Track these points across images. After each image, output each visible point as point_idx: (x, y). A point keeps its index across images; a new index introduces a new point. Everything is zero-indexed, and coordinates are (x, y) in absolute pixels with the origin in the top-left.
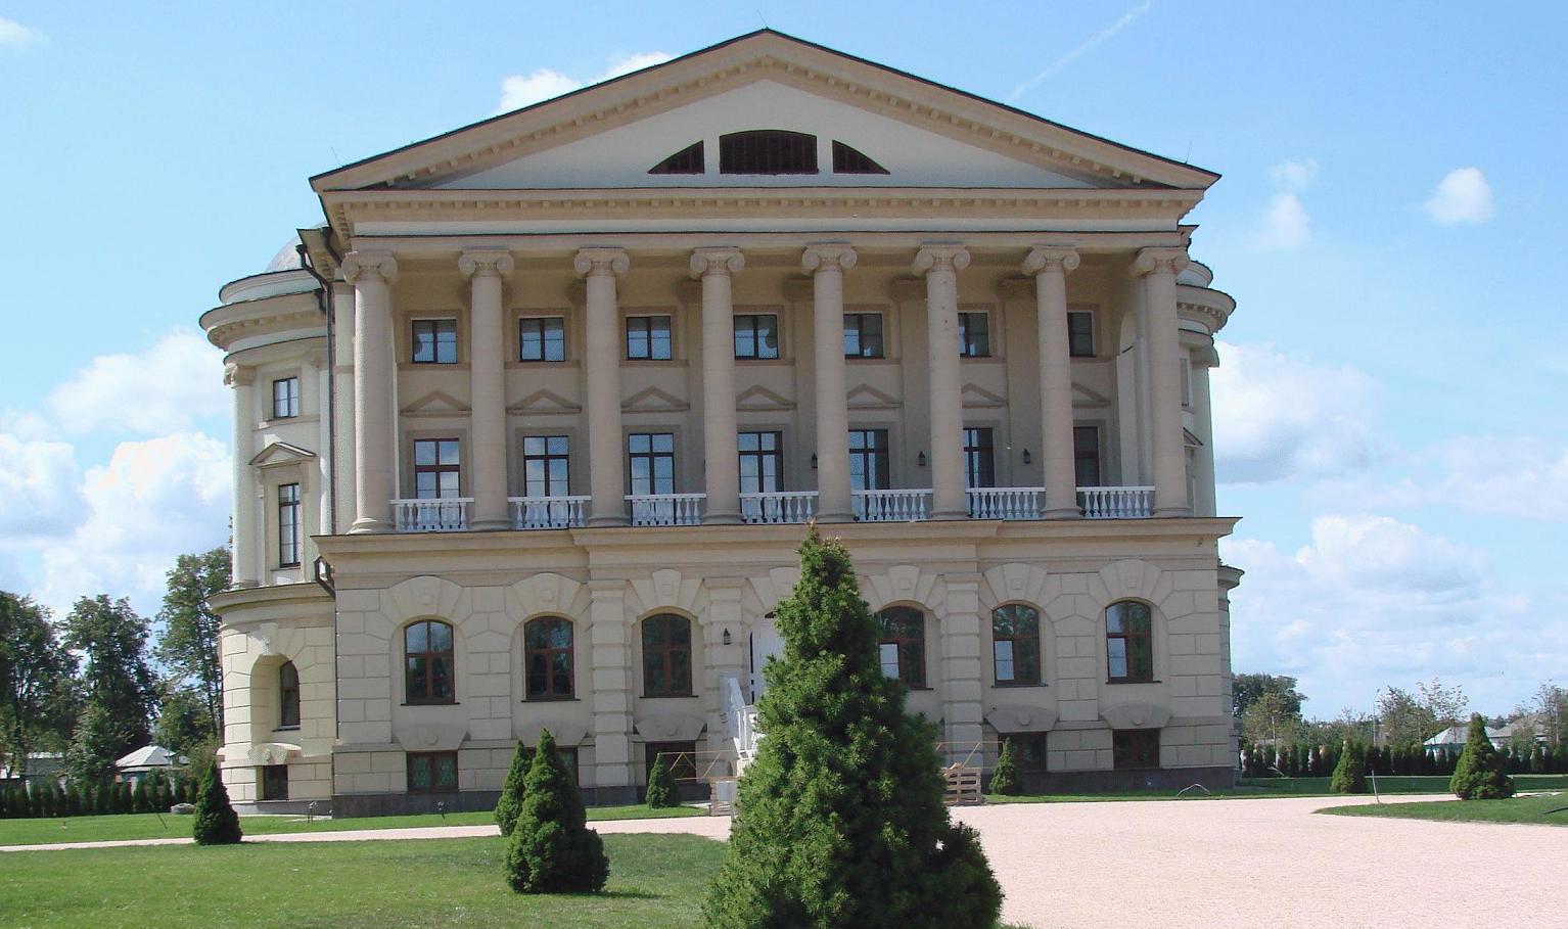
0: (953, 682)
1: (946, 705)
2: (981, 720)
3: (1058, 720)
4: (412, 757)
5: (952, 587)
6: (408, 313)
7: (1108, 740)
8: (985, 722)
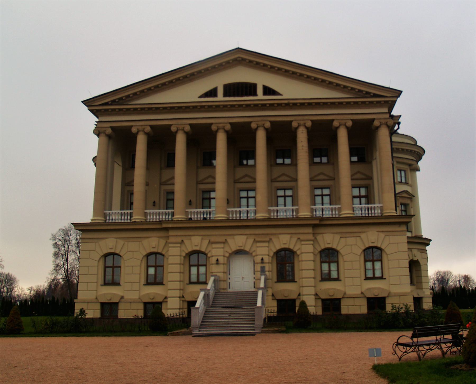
0: (304, 279)
1: (301, 288)
2: (314, 293)
3: (345, 294)
4: (103, 304)
5: (303, 243)
8: (316, 295)
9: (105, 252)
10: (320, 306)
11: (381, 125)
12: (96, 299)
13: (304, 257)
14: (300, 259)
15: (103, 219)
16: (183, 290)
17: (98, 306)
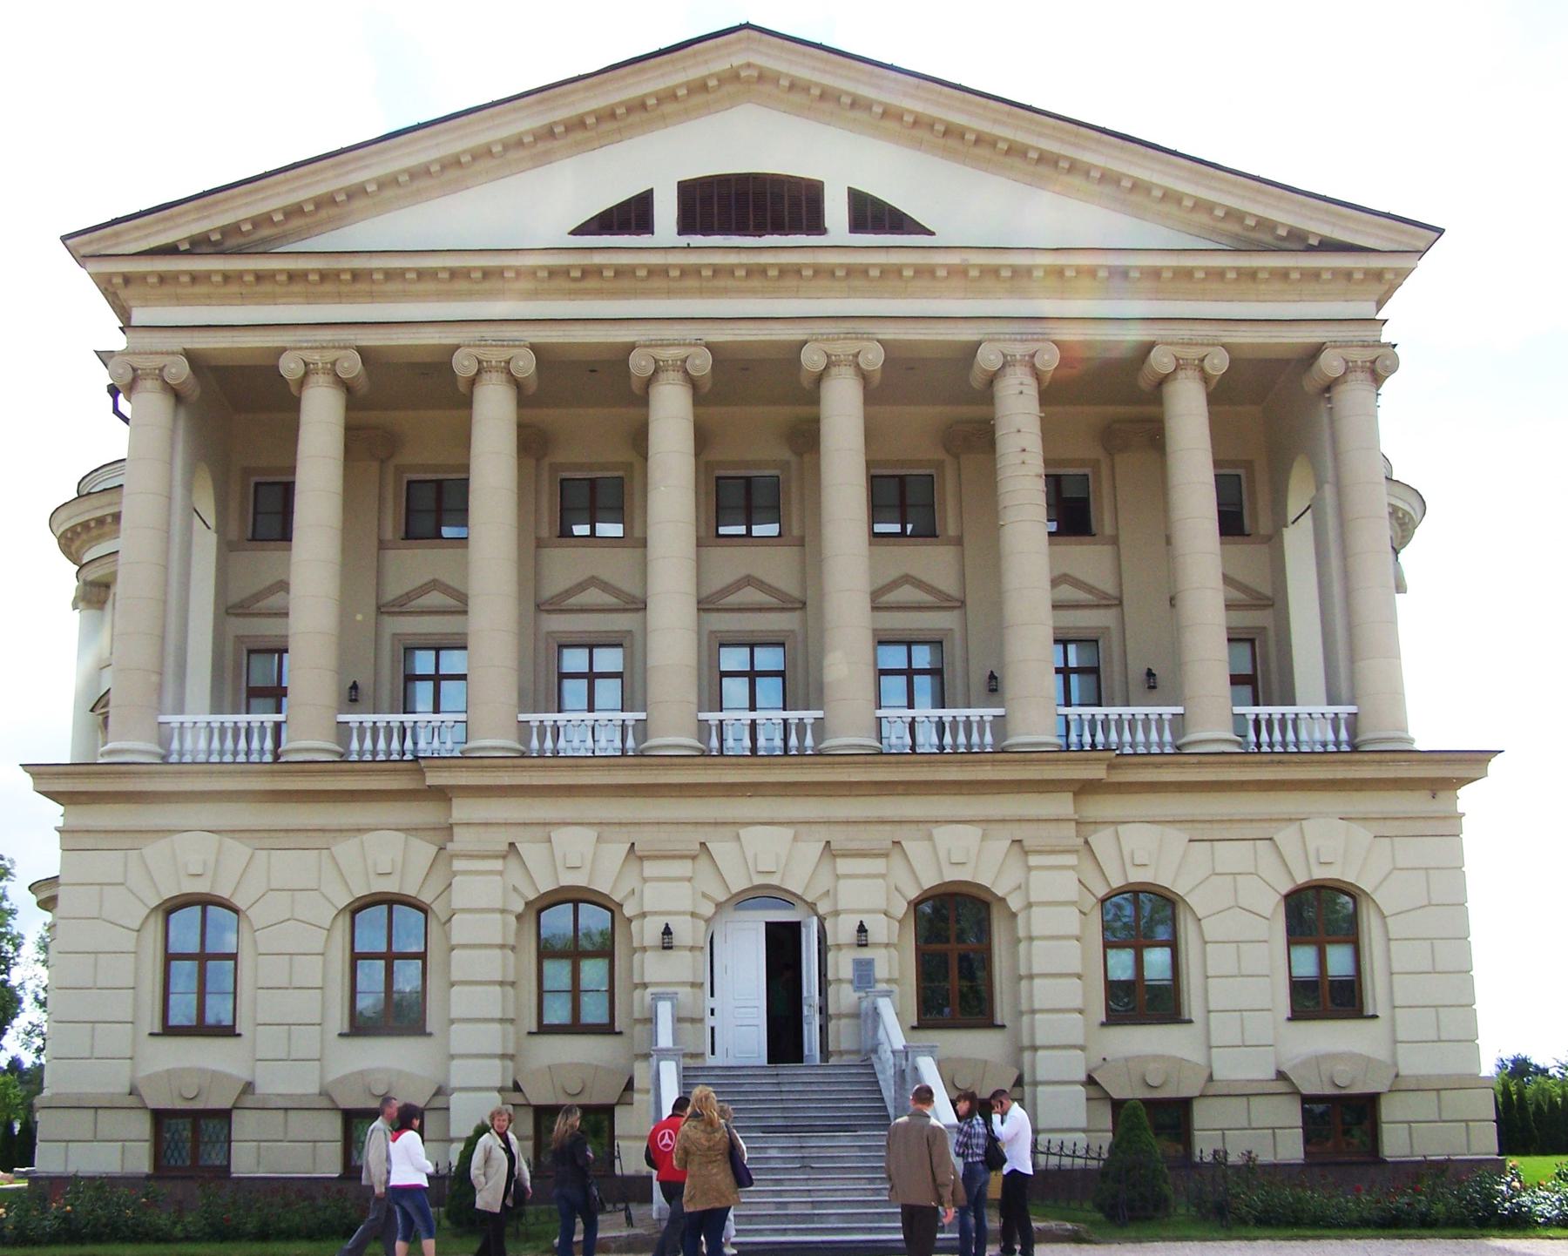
2: (1083, 1077)
3: (1211, 1078)
6: (247, 472)
7: (1292, 1114)
8: (1091, 1081)
9: (170, 891)
10: (1107, 1131)
11: (1347, 370)
12: (130, 1094)
13: (1040, 922)
14: (1021, 933)
15: (157, 749)
16: (511, 1057)
17: (142, 1126)
